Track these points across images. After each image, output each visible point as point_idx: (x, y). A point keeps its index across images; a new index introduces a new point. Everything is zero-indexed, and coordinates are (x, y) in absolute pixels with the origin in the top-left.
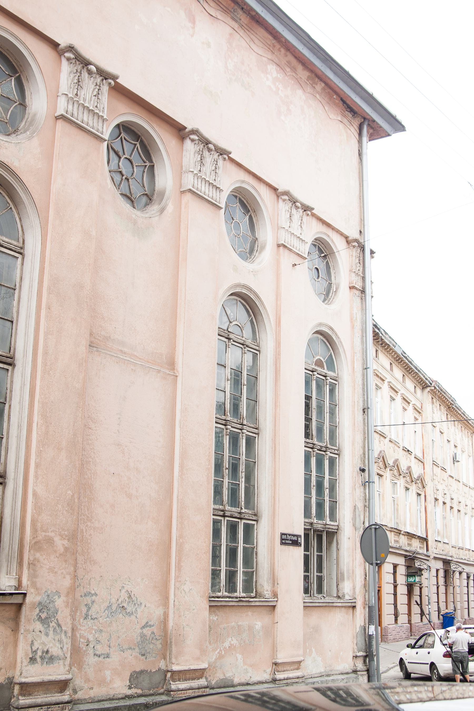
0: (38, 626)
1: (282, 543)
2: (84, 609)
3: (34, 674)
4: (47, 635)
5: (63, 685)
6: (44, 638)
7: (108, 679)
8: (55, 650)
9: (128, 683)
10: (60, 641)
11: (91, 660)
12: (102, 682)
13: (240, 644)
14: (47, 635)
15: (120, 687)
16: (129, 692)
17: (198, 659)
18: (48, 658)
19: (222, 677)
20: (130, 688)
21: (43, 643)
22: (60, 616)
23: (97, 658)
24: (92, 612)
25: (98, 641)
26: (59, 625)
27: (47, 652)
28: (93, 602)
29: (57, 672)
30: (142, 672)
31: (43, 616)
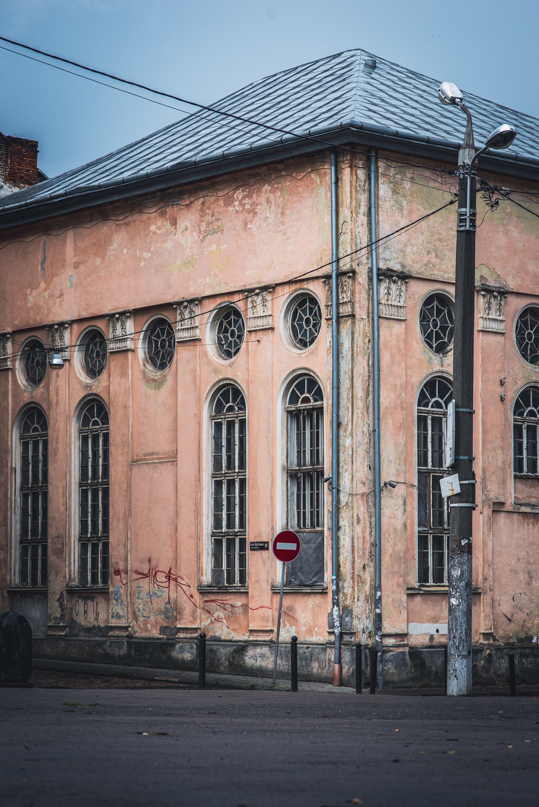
0: (114, 602)
1: (251, 550)
2: (137, 594)
3: (113, 622)
4: (118, 606)
5: (126, 628)
6: (116, 607)
7: (149, 629)
8: (121, 613)
9: (159, 632)
10: (123, 609)
11: (141, 619)
12: (146, 630)
13: (225, 616)
14: (118, 606)
15: (155, 633)
16: (160, 636)
17: (192, 622)
18: (119, 617)
19: (213, 635)
20: (160, 634)
21: (116, 610)
22: (122, 597)
23: (144, 618)
24: (141, 595)
25: (144, 610)
26: (122, 602)
27: (118, 613)
28: (141, 591)
29: (123, 623)
30: (166, 627)
31: (116, 597)
